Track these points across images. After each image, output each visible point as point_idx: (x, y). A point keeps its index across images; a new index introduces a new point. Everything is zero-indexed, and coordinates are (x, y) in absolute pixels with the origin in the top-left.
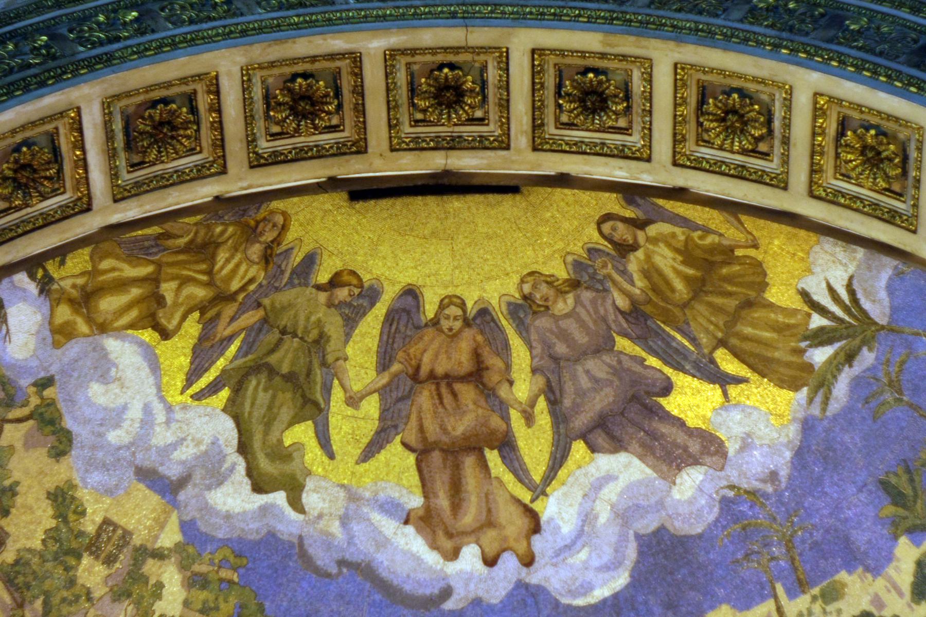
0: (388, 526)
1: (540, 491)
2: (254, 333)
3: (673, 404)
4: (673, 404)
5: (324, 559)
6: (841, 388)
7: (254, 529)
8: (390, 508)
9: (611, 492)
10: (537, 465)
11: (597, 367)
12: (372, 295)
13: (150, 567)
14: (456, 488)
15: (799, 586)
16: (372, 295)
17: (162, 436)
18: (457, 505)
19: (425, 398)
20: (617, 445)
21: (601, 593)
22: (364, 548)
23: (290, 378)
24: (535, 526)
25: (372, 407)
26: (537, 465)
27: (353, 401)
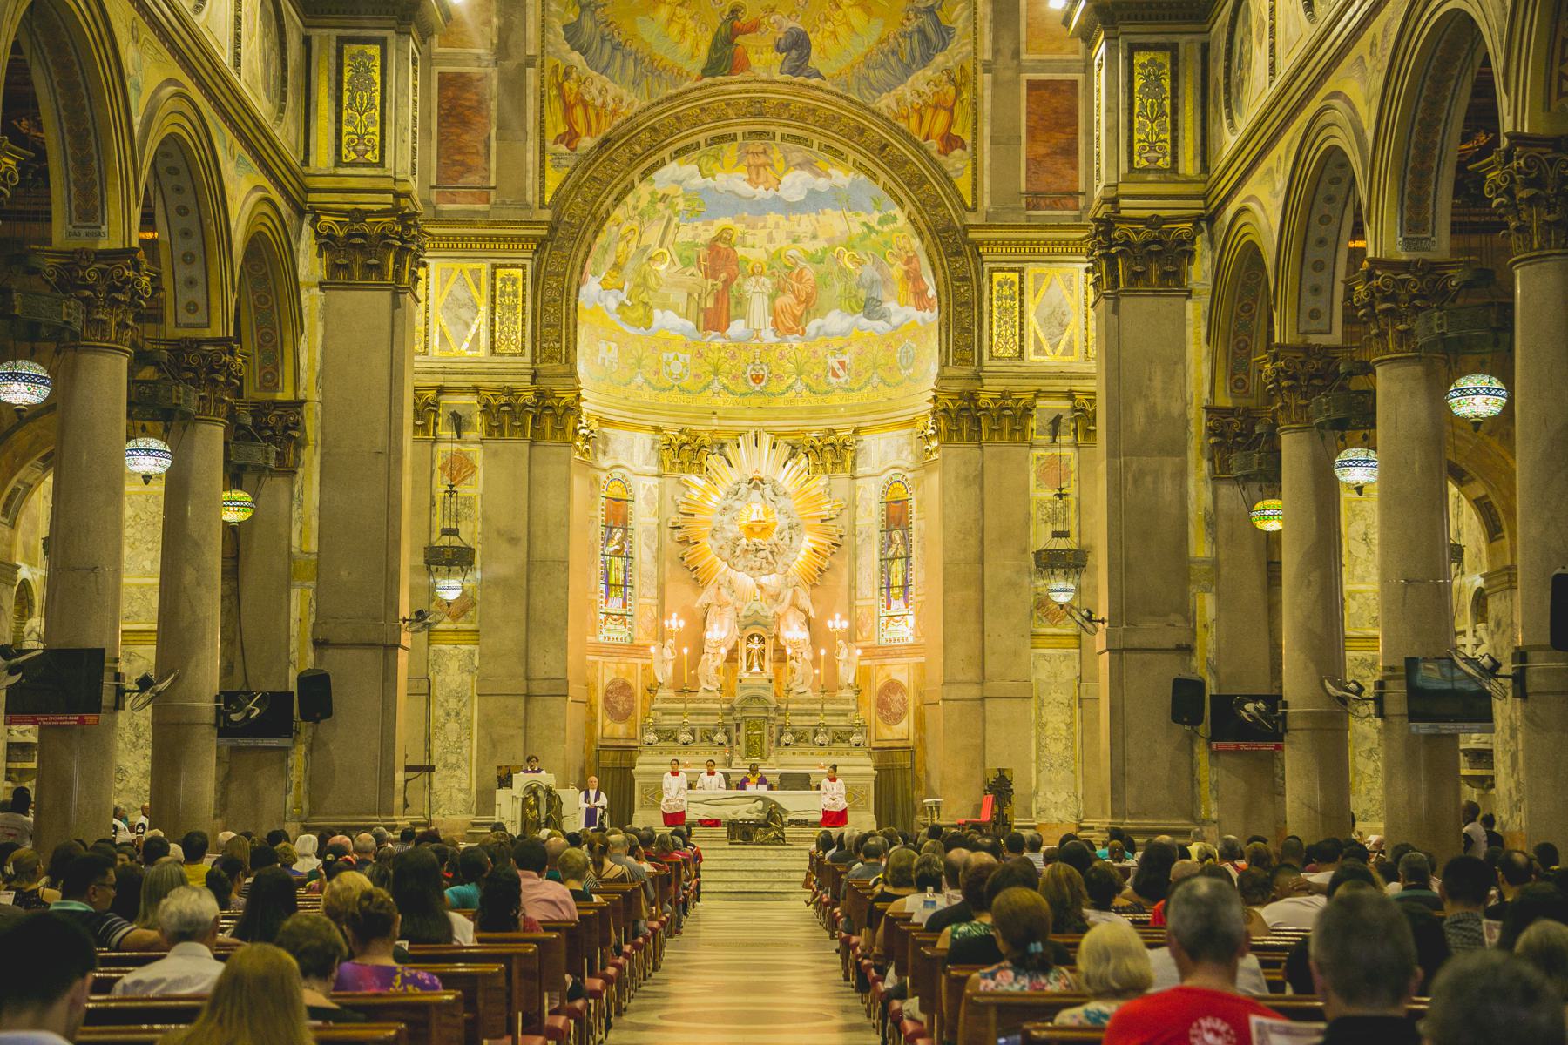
13: (675, 200)
14: (758, 174)
17: (678, 173)
20: (802, 169)
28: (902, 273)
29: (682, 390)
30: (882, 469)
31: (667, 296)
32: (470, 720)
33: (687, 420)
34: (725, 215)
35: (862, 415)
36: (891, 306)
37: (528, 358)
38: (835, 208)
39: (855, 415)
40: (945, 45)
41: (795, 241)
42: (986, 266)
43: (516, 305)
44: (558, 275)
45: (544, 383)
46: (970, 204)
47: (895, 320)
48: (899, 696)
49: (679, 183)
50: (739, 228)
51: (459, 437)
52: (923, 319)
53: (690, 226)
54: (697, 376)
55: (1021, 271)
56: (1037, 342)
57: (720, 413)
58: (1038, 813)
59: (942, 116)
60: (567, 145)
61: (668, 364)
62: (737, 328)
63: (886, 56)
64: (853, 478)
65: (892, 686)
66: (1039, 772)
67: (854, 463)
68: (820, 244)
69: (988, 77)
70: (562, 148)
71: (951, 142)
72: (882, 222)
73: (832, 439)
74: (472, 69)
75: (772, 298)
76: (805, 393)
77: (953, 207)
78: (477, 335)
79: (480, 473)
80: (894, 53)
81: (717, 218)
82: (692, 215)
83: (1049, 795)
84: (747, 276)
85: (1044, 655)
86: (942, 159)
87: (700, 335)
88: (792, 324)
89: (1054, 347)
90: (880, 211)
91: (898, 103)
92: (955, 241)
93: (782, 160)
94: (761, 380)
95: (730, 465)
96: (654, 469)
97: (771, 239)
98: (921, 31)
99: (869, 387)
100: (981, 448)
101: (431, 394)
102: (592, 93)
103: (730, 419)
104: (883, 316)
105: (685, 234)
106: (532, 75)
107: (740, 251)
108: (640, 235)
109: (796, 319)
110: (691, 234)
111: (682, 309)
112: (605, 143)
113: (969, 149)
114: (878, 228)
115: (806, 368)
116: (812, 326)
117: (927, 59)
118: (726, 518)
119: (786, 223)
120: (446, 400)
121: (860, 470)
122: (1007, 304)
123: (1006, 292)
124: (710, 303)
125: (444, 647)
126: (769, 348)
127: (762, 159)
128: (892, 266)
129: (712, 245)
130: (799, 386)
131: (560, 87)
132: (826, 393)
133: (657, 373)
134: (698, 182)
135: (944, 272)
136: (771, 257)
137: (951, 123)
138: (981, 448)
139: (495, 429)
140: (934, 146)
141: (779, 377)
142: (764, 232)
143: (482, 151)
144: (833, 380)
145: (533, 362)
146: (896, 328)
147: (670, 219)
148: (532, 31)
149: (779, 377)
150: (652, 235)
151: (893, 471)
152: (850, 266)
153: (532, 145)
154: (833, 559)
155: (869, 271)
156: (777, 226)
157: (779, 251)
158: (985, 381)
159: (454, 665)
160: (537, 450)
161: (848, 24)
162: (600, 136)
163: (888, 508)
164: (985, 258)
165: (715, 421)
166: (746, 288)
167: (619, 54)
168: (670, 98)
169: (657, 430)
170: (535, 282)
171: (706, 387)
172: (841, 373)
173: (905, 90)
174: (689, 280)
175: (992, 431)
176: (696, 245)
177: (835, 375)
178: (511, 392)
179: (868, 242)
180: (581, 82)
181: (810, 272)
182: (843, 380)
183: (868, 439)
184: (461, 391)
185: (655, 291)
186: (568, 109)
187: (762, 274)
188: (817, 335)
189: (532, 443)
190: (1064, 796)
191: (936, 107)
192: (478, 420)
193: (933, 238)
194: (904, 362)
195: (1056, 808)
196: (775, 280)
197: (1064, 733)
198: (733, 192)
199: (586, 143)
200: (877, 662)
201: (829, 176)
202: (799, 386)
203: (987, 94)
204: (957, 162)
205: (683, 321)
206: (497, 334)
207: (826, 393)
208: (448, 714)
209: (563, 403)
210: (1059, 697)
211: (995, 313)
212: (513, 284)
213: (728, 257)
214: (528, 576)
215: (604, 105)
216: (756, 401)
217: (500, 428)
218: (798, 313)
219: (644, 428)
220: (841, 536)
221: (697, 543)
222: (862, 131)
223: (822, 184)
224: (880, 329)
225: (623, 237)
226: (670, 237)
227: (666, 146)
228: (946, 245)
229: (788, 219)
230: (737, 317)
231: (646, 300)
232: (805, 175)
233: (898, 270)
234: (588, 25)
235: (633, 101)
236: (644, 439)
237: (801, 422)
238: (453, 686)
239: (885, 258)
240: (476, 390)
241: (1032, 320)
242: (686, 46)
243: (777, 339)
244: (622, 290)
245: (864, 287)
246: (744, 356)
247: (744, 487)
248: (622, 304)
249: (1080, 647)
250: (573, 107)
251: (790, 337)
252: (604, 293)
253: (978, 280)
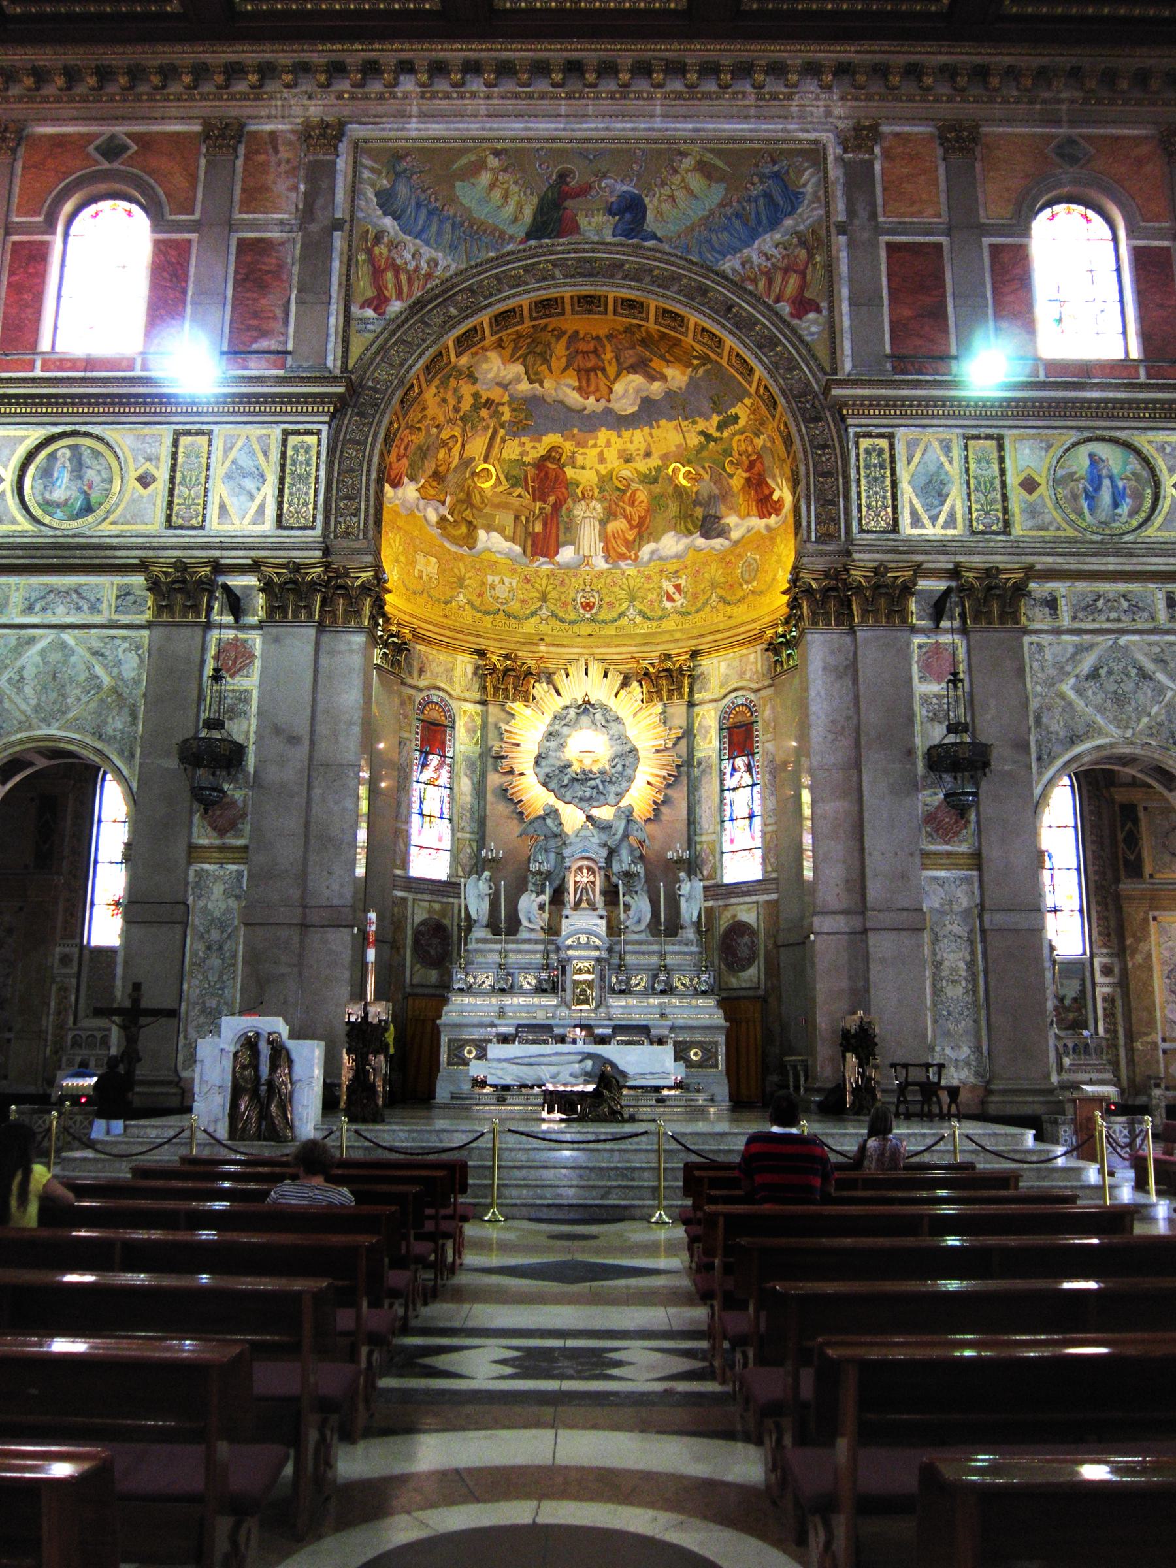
0: (568, 391)
1: (613, 382)
2: (529, 345)
3: (652, 364)
4: (652, 364)
5: (549, 400)
6: (701, 371)
7: (529, 394)
8: (568, 386)
9: (634, 385)
10: (612, 375)
11: (631, 352)
12: (565, 333)
13: (501, 408)
14: (588, 380)
15: (686, 419)
16: (565, 333)
17: (503, 373)
18: (588, 385)
19: (580, 357)
20: (636, 373)
21: (630, 411)
22: (561, 397)
23: (541, 354)
24: (611, 391)
25: (564, 360)
26: (612, 375)
27: (558, 359)
28: (742, 481)
29: (508, 615)
30: (723, 692)
31: (493, 517)
32: (234, 956)
33: (512, 646)
34: (554, 432)
35: (699, 637)
36: (731, 520)
37: (319, 531)
38: (671, 419)
39: (692, 638)
40: (793, 210)
41: (627, 461)
42: (851, 431)
43: (309, 474)
44: (358, 443)
45: (337, 561)
46: (828, 369)
47: (735, 535)
48: (746, 939)
49: (504, 386)
50: (569, 446)
51: (237, 620)
52: (768, 527)
53: (517, 441)
54: (523, 601)
55: (891, 437)
56: (914, 513)
57: (548, 640)
59: (793, 281)
60: (375, 310)
61: (493, 587)
62: (566, 554)
63: (730, 219)
64: (691, 705)
65: (738, 928)
66: (935, 1022)
67: (691, 692)
68: (654, 462)
69: (842, 239)
70: (370, 313)
71: (803, 306)
72: (721, 427)
73: (669, 664)
74: (274, 234)
75: (603, 523)
76: (638, 619)
77: (811, 370)
78: (261, 509)
79: (257, 663)
80: (738, 216)
81: (545, 434)
82: (518, 429)
83: (948, 1051)
84: (577, 500)
85: (936, 878)
86: (795, 322)
87: (525, 560)
88: (623, 550)
89: (934, 519)
90: (719, 413)
91: (743, 264)
92: (813, 406)
93: (614, 361)
94: (592, 608)
95: (559, 694)
96: (477, 696)
97: (602, 460)
98: (767, 195)
99: (708, 608)
100: (852, 631)
101: (205, 571)
102: (405, 257)
103: (558, 646)
104: (723, 533)
105: (512, 450)
106: (339, 241)
107: (570, 472)
108: (463, 445)
109: (628, 544)
110: (518, 450)
111: (509, 531)
112: (418, 306)
113: (825, 313)
114: (717, 434)
115: (639, 594)
116: (646, 550)
117: (774, 224)
118: (552, 745)
119: (619, 440)
120: (221, 579)
121: (698, 697)
122: (876, 473)
123: (875, 460)
124: (538, 528)
125: (206, 866)
126: (600, 575)
127: (592, 361)
128: (731, 476)
129: (540, 463)
130: (632, 613)
131: (369, 252)
132: (660, 618)
133: (481, 595)
134: (524, 387)
135: (802, 440)
136: (602, 479)
137: (803, 286)
138: (852, 631)
139: (277, 613)
140: (785, 308)
141: (611, 605)
142: (593, 453)
143: (279, 313)
144: (668, 605)
145: (325, 536)
146: (736, 543)
147: (495, 433)
148: (340, 196)
149: (611, 605)
150: (477, 446)
151: (734, 695)
152: (684, 483)
153: (336, 307)
154: (669, 792)
155: (706, 486)
156: (608, 444)
157: (611, 473)
158: (856, 556)
159: (218, 889)
160: (326, 639)
161: (687, 188)
162: (410, 301)
163: (730, 735)
164: (849, 421)
165: (543, 648)
166: (576, 512)
167: (435, 219)
168: (492, 260)
169: (481, 654)
170: (331, 452)
171: (533, 614)
172: (676, 596)
173: (752, 252)
174: (517, 502)
175: (865, 613)
176: (524, 464)
177: (670, 599)
178: (297, 567)
179: (705, 454)
180: (394, 245)
181: (642, 496)
182: (678, 604)
183: (706, 664)
184: (241, 569)
185: (480, 510)
186: (377, 273)
187: (592, 498)
188: (650, 560)
189: (321, 628)
191: (786, 270)
192: (261, 600)
193: (788, 402)
194: (746, 577)
195: (956, 1067)
196: (606, 504)
197: (964, 974)
198: (561, 403)
199: (396, 307)
200: (721, 903)
201: (664, 378)
202: (632, 613)
203: (843, 255)
204: (811, 325)
205: (508, 544)
206: (286, 506)
207: (660, 618)
208: (209, 948)
209: (359, 582)
210: (956, 929)
211: (863, 482)
212: (307, 452)
213: (557, 477)
214: (309, 783)
215: (417, 268)
216: (586, 629)
217: (283, 609)
218: (631, 538)
219: (464, 651)
220: (678, 767)
221: (522, 774)
222: (703, 291)
223: (656, 388)
224: (718, 547)
225: (444, 444)
226: (495, 451)
227: (485, 307)
228: (803, 411)
229: (620, 436)
230: (564, 544)
231: (470, 518)
232: (637, 380)
233: (737, 481)
234: (402, 190)
235: (448, 264)
236: (464, 664)
237: (635, 649)
238: (217, 914)
239: (724, 469)
240: (255, 566)
241: (907, 492)
242: (510, 209)
243: (606, 566)
244: (443, 503)
245: (701, 505)
246: (576, 583)
247: (572, 712)
248: (443, 519)
249: (979, 867)
250: (383, 271)
251: (622, 564)
252: (422, 503)
253: (842, 448)
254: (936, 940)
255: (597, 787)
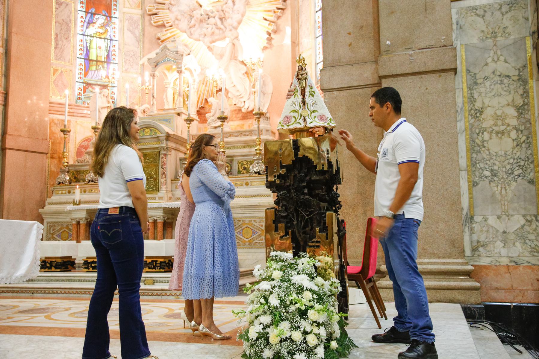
58: (474, 250)
83: (492, 221)
154: (279, 22)
190: (518, 221)
197: (514, 122)
210: (501, 67)
254: (473, 84)
255: (216, 24)
